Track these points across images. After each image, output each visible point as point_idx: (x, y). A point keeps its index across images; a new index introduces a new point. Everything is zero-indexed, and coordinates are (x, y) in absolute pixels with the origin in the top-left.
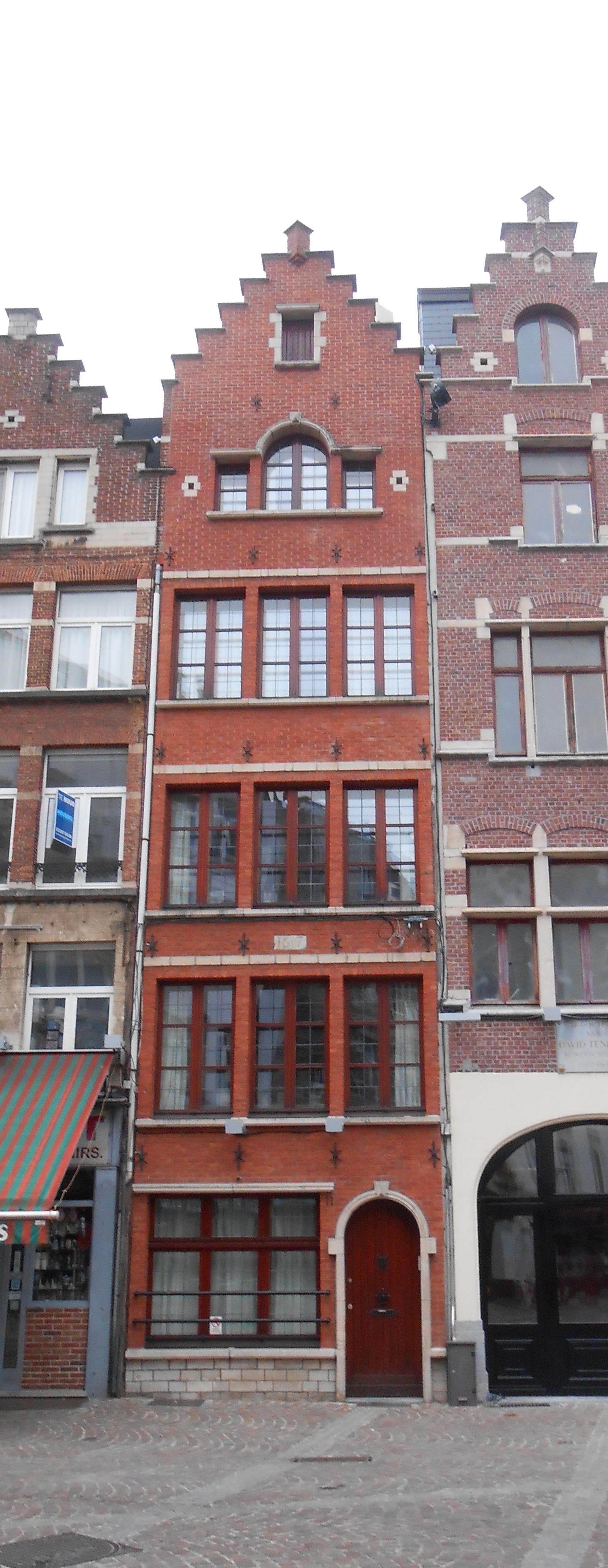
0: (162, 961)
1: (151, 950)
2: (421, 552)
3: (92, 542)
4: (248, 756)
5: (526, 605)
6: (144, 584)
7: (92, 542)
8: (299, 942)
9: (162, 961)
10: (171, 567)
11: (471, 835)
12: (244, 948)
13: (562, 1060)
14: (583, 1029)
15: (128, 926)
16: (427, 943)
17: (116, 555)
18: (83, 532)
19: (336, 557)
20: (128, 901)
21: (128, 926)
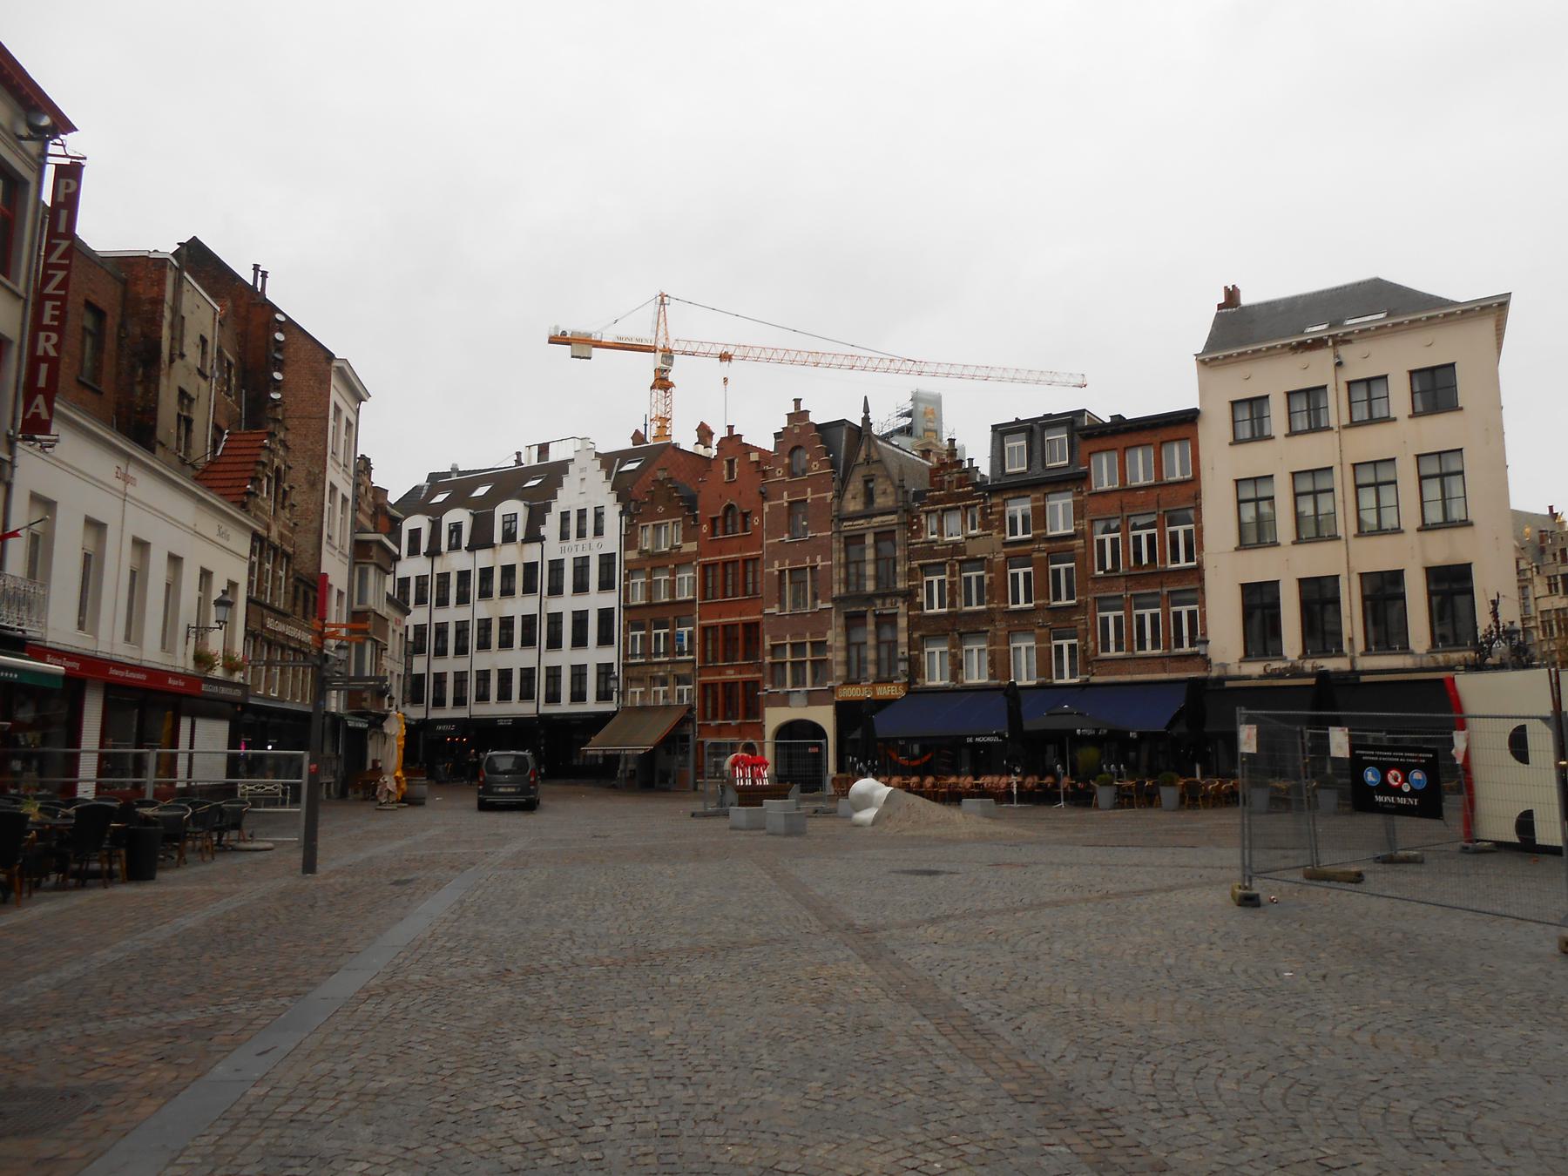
0: (702, 679)
1: (700, 676)
2: (762, 546)
3: (682, 551)
4: (720, 618)
5: (787, 562)
6: (694, 563)
7: (682, 551)
8: (732, 672)
9: (702, 679)
10: (701, 557)
11: (772, 638)
12: (720, 675)
13: (791, 704)
14: (797, 694)
15: (694, 668)
16: (760, 672)
17: (688, 554)
18: (679, 547)
19: (740, 550)
20: (693, 661)
21: (694, 668)
